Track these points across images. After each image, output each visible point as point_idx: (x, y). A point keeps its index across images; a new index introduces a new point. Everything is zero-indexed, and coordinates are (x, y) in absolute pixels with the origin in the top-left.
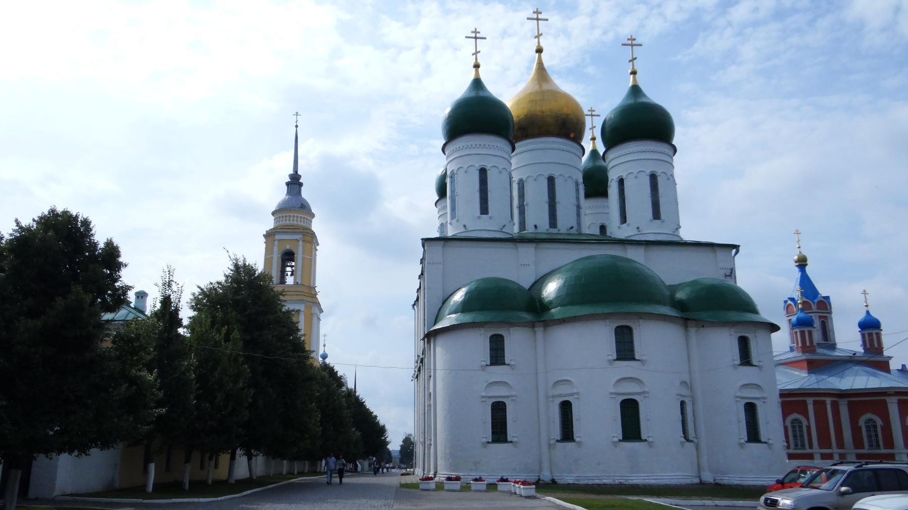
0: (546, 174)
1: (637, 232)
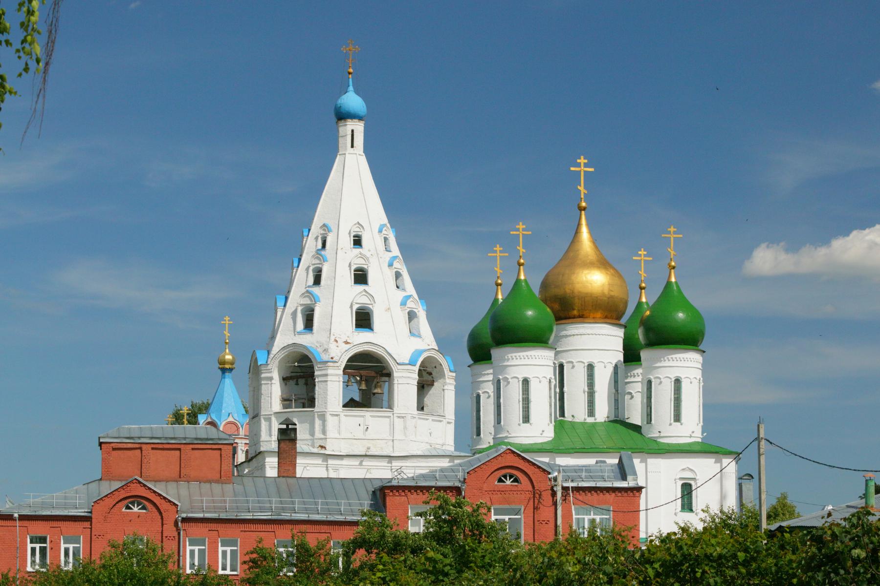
0: (586, 362)
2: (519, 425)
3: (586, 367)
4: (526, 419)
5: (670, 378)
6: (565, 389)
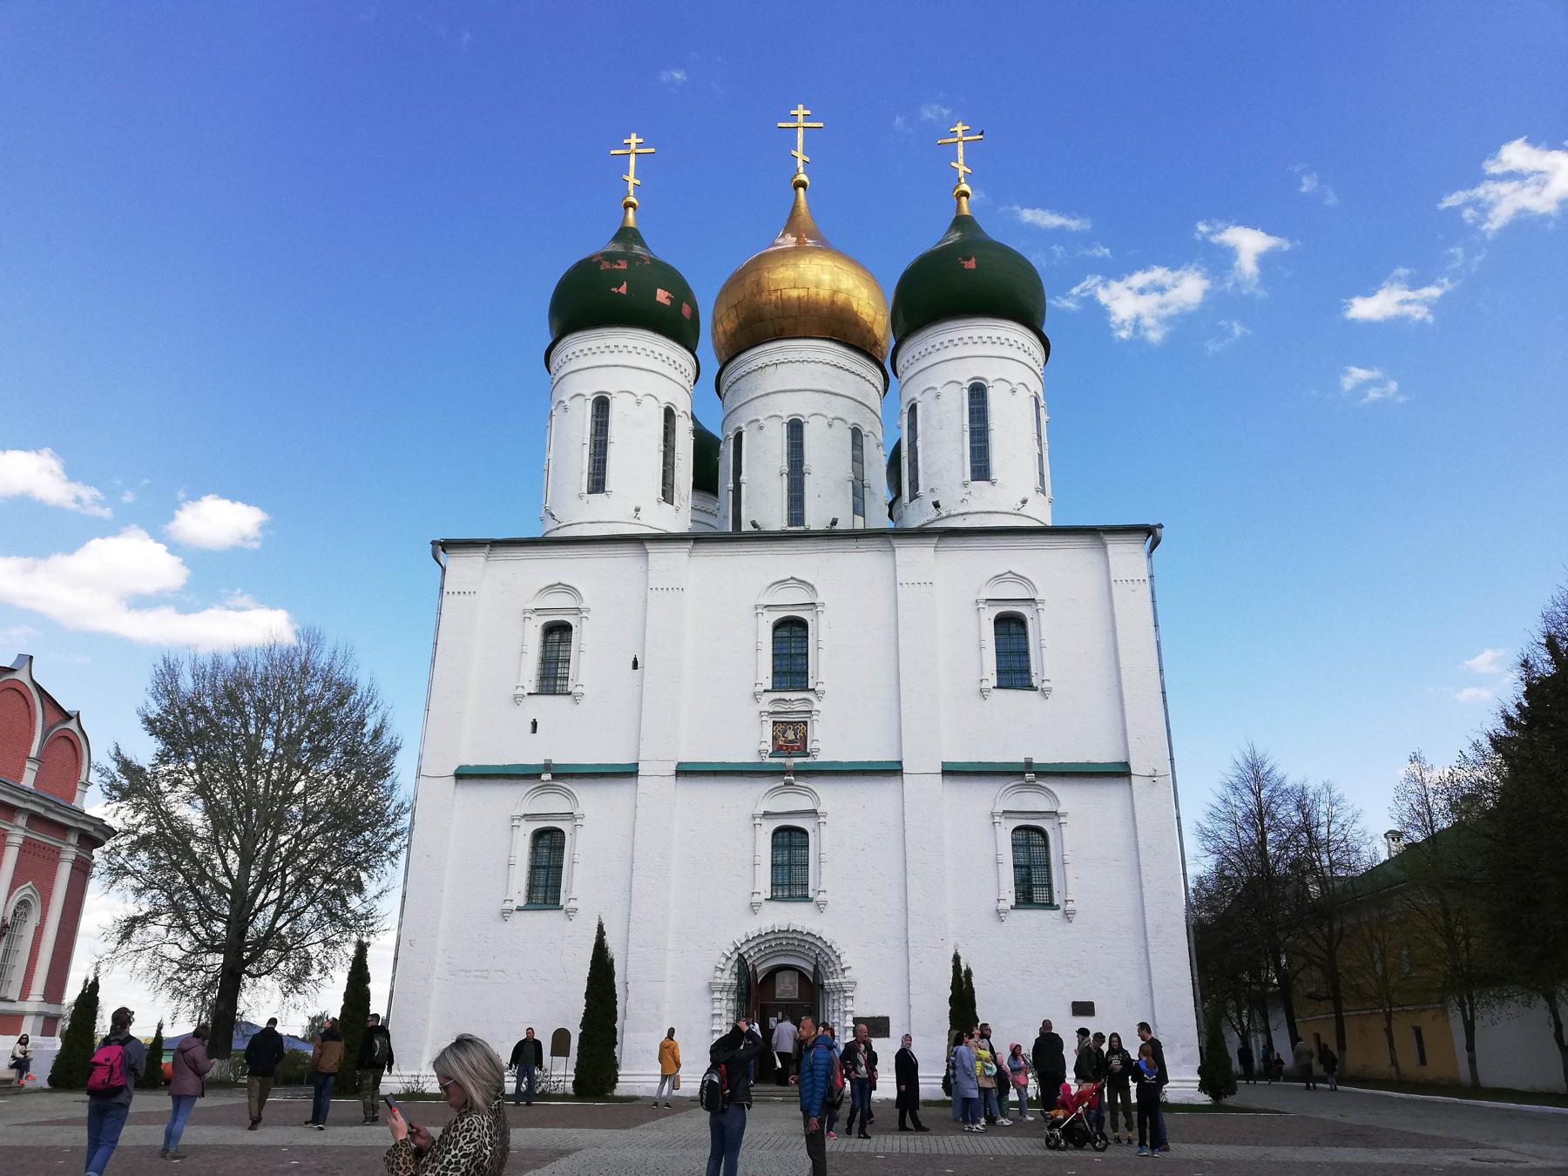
2: (580, 497)
4: (597, 484)
6: (743, 478)
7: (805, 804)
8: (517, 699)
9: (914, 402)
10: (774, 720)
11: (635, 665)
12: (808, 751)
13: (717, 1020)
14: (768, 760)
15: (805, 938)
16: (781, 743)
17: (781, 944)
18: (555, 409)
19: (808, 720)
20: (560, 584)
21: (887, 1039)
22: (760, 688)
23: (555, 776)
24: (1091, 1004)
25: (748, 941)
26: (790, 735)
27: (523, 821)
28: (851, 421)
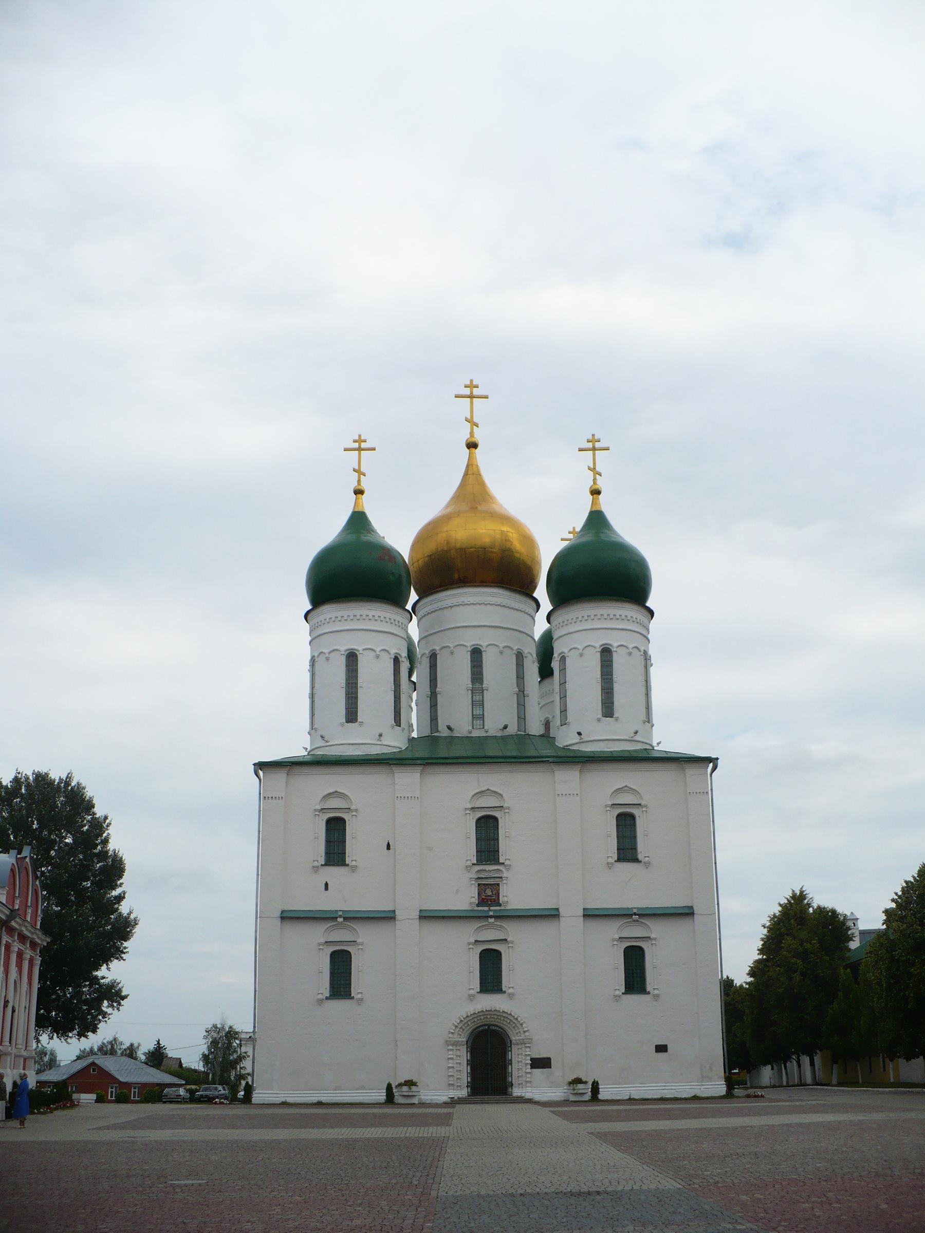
0: (470, 643)
1: (576, 739)
3: (469, 653)
4: (352, 716)
5: (595, 647)
7: (501, 936)
8: (315, 869)
9: (563, 654)
10: (479, 883)
11: (388, 847)
12: (501, 902)
13: (451, 1061)
14: (476, 908)
15: (501, 1014)
16: (483, 897)
17: (487, 1018)
18: (318, 656)
19: (500, 883)
20: (336, 792)
21: (549, 1069)
22: (469, 863)
23: (345, 919)
24: (666, 1046)
25: (467, 1016)
26: (489, 892)
27: (325, 946)
28: (515, 648)
